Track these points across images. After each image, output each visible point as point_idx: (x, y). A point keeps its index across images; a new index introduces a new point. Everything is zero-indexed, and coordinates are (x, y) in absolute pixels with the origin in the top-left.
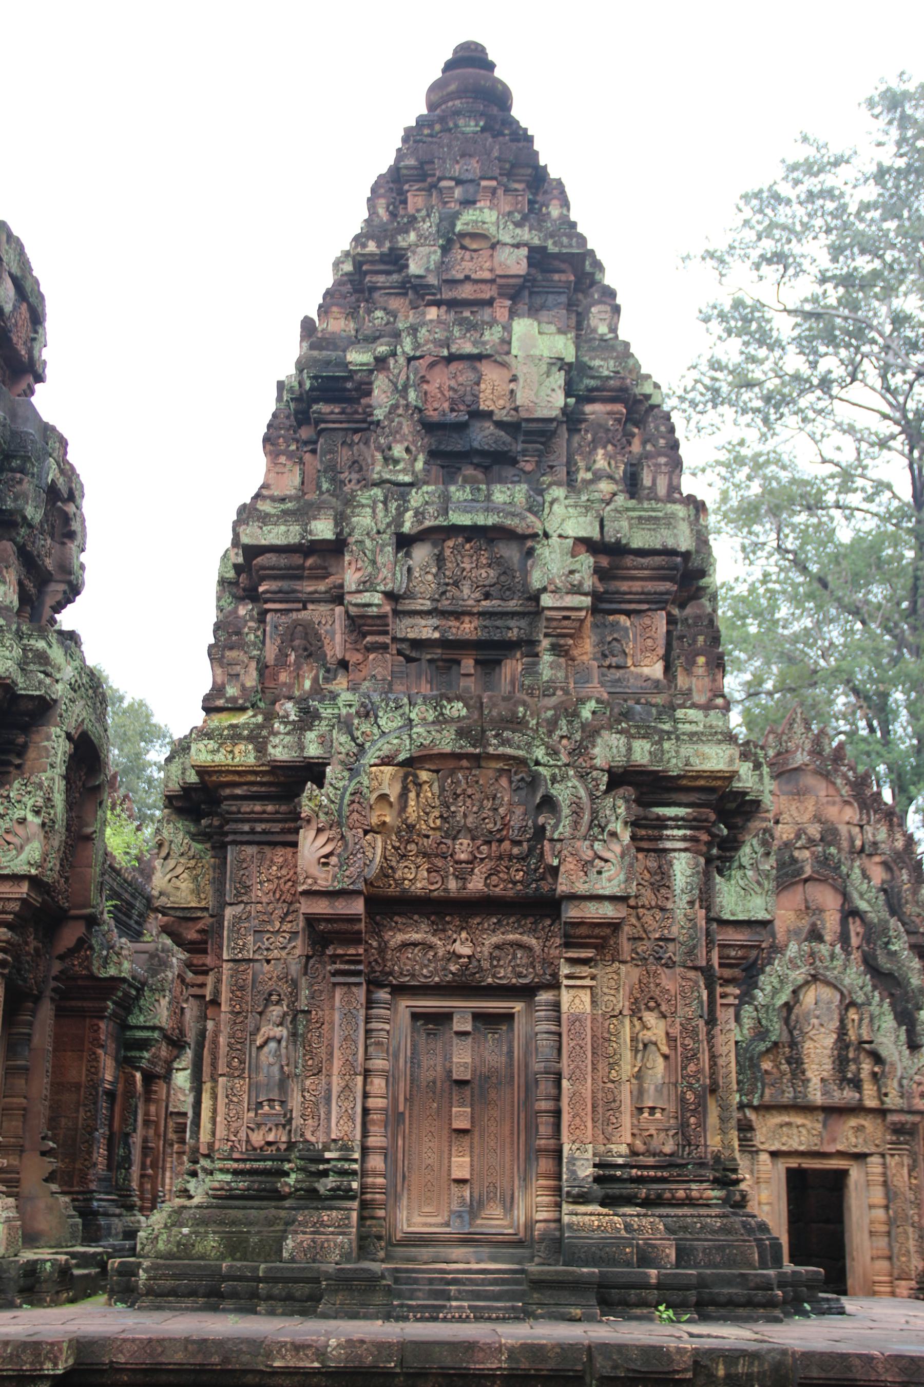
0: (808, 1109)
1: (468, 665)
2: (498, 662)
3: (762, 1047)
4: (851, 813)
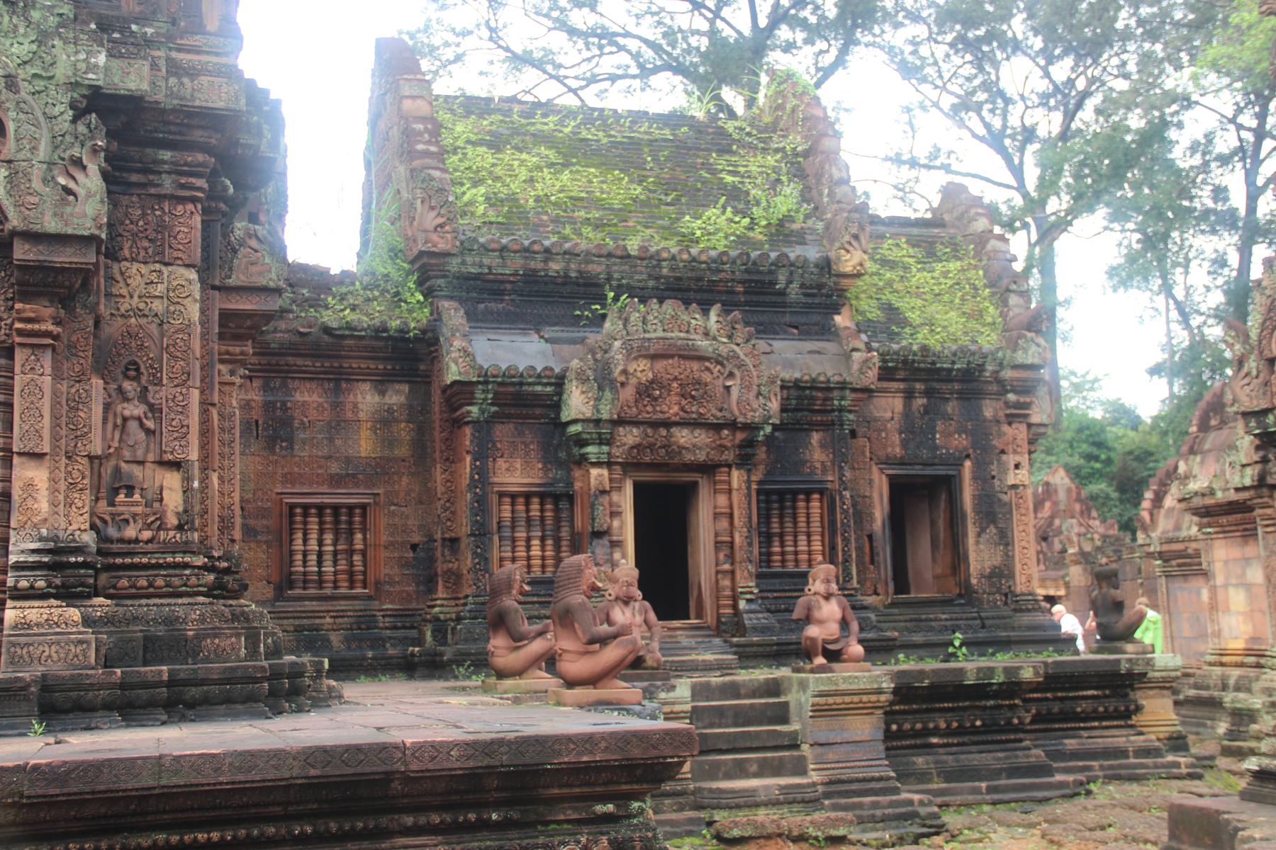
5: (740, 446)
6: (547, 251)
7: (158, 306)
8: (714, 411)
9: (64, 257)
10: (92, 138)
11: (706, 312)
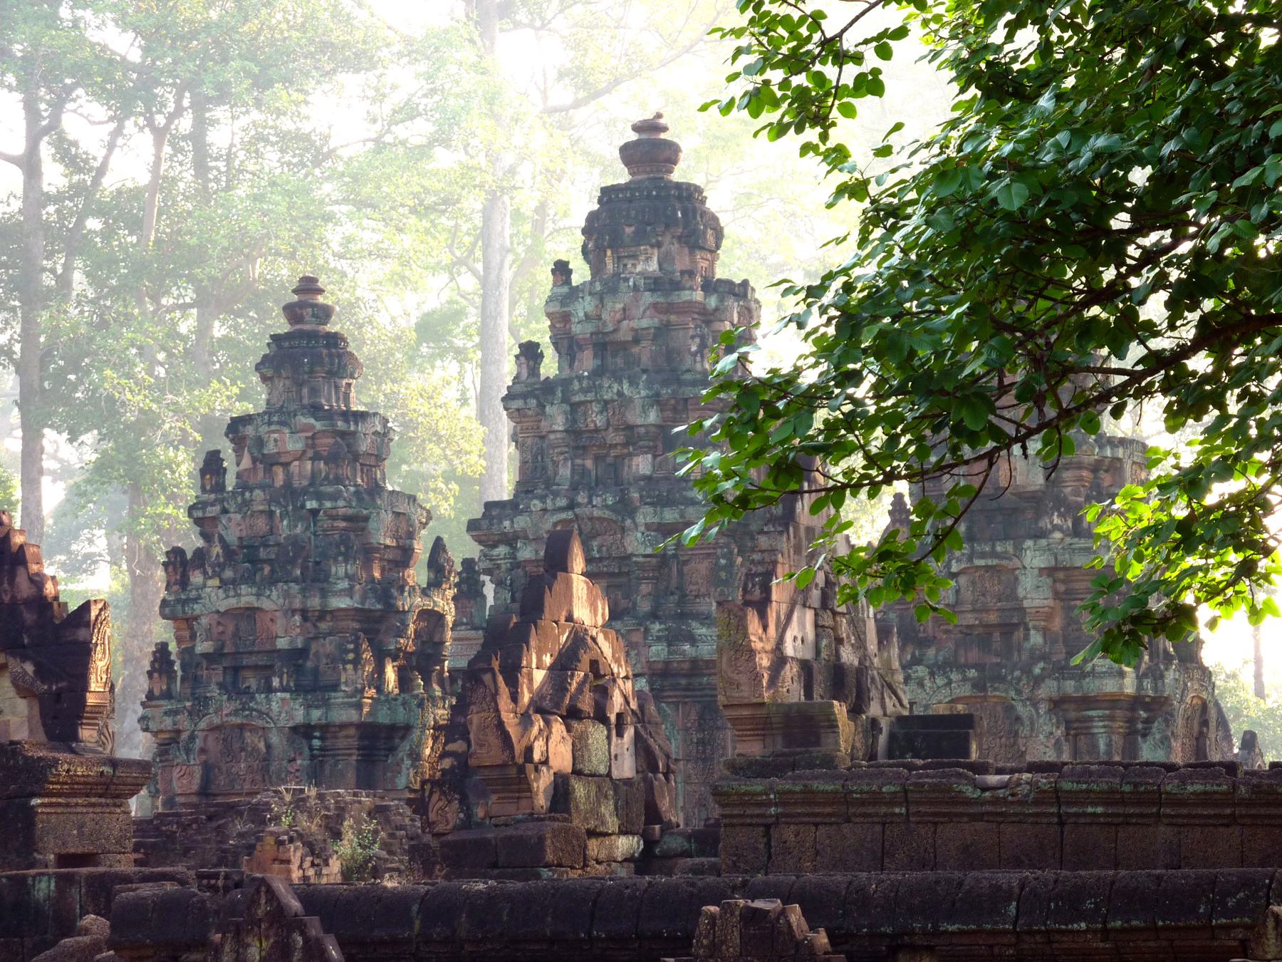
1: (996, 635)
2: (1012, 633)
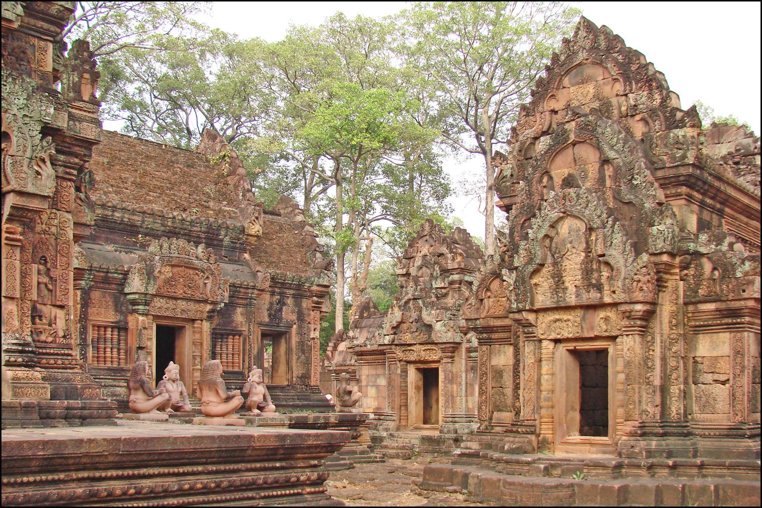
0: (568, 308)
3: (530, 269)
4: (619, 87)
5: (208, 312)
6: (114, 207)
7: (54, 229)
8: (199, 294)
9: (35, 204)
10: (50, 149)
11: (197, 247)
